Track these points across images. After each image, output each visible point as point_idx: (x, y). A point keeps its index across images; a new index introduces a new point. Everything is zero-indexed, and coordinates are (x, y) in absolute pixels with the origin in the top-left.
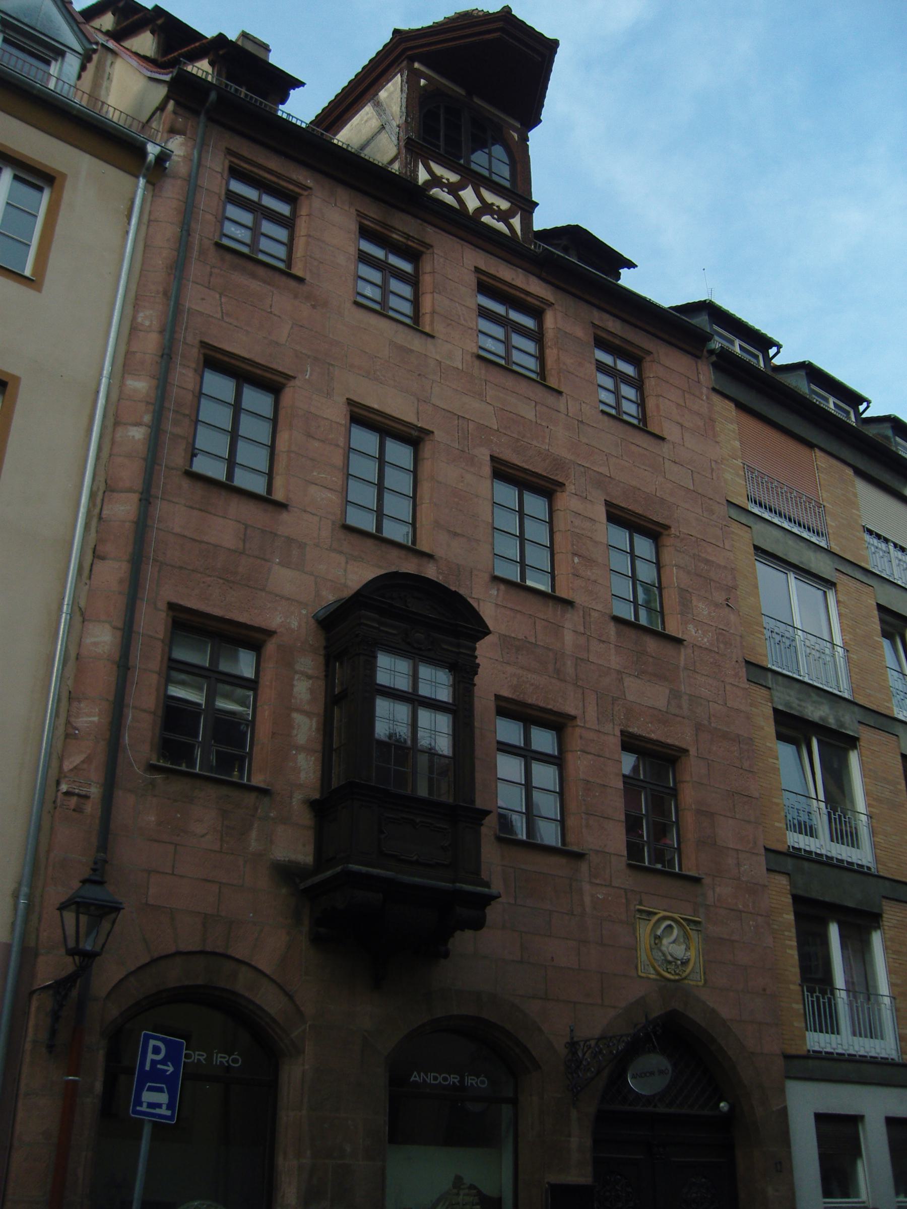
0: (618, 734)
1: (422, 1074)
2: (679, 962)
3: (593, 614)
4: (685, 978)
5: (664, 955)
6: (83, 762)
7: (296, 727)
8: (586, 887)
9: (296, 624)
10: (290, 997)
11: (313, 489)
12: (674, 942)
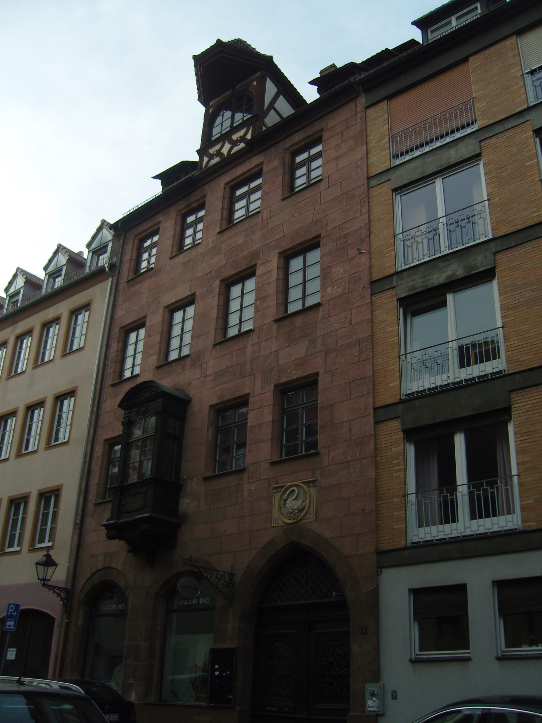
1: (183, 601)
4: (301, 519)
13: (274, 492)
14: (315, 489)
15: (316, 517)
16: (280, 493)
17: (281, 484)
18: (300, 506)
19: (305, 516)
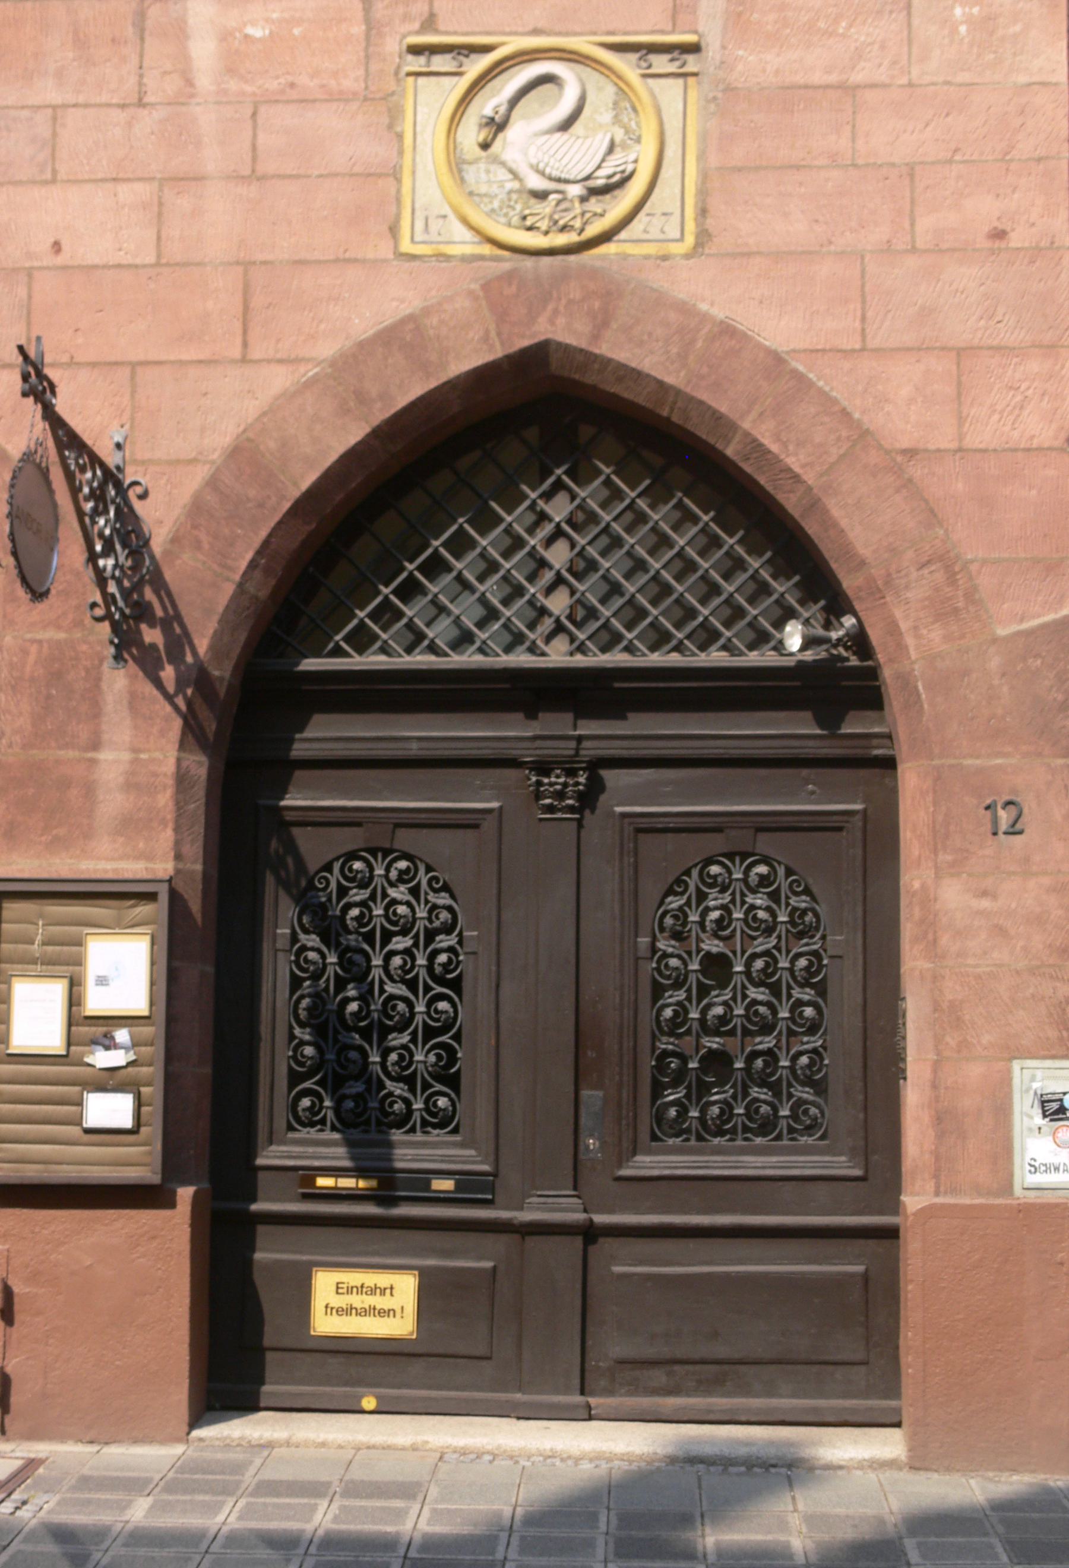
2: (575, 190)
4: (605, 237)
5: (515, 175)
12: (566, 125)
13: (409, 74)
14: (693, 95)
15: (703, 237)
16: (464, 82)
17: (447, 33)
18: (599, 167)
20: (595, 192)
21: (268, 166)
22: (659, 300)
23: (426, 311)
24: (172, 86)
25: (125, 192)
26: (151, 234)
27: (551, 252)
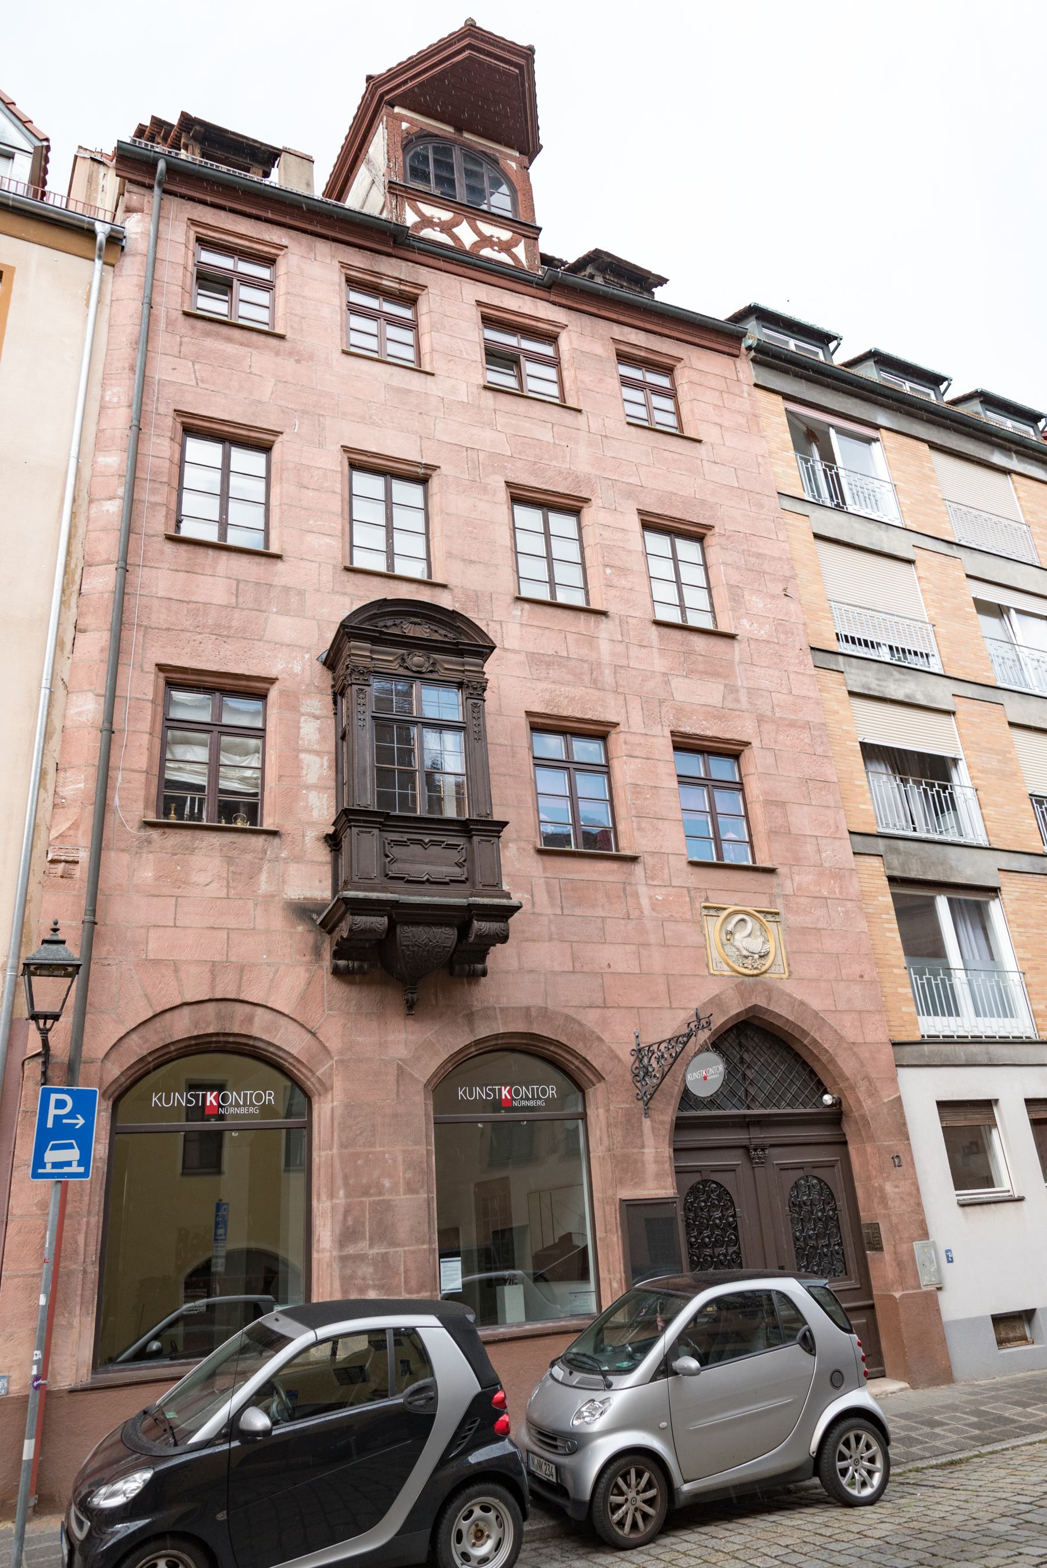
0: (669, 735)
2: (756, 956)
3: (630, 620)
4: (765, 972)
5: (738, 950)
6: (69, 828)
7: (305, 767)
8: (643, 890)
9: (299, 668)
10: (314, 1034)
11: (310, 538)
12: (749, 935)
19: (770, 967)
20: (761, 957)
21: (669, 942)
22: (783, 993)
23: (721, 993)
24: (637, 913)
25: (627, 947)
26: (637, 963)
27: (753, 976)
